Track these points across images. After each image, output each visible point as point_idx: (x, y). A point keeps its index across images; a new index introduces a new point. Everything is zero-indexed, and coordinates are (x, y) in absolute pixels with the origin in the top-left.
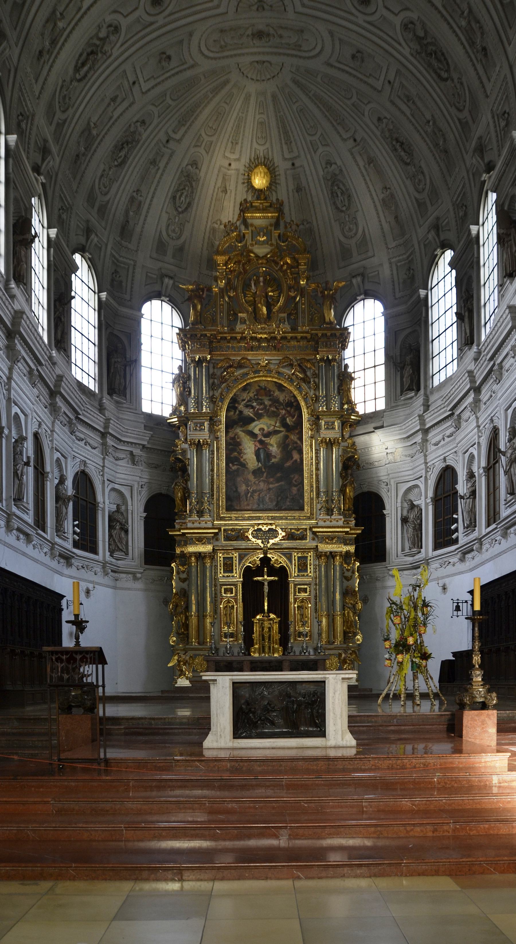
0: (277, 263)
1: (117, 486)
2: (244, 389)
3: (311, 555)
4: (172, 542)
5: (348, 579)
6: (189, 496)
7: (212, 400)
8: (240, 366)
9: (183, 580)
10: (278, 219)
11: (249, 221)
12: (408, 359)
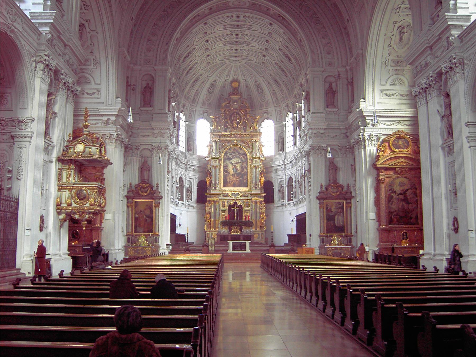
0: (240, 111)
1: (189, 179)
2: (229, 149)
3: (249, 201)
4: (206, 197)
5: (261, 209)
6: (212, 183)
7: (219, 153)
8: (228, 143)
9: (210, 209)
10: (240, 98)
11: (232, 98)
12: (280, 141)
